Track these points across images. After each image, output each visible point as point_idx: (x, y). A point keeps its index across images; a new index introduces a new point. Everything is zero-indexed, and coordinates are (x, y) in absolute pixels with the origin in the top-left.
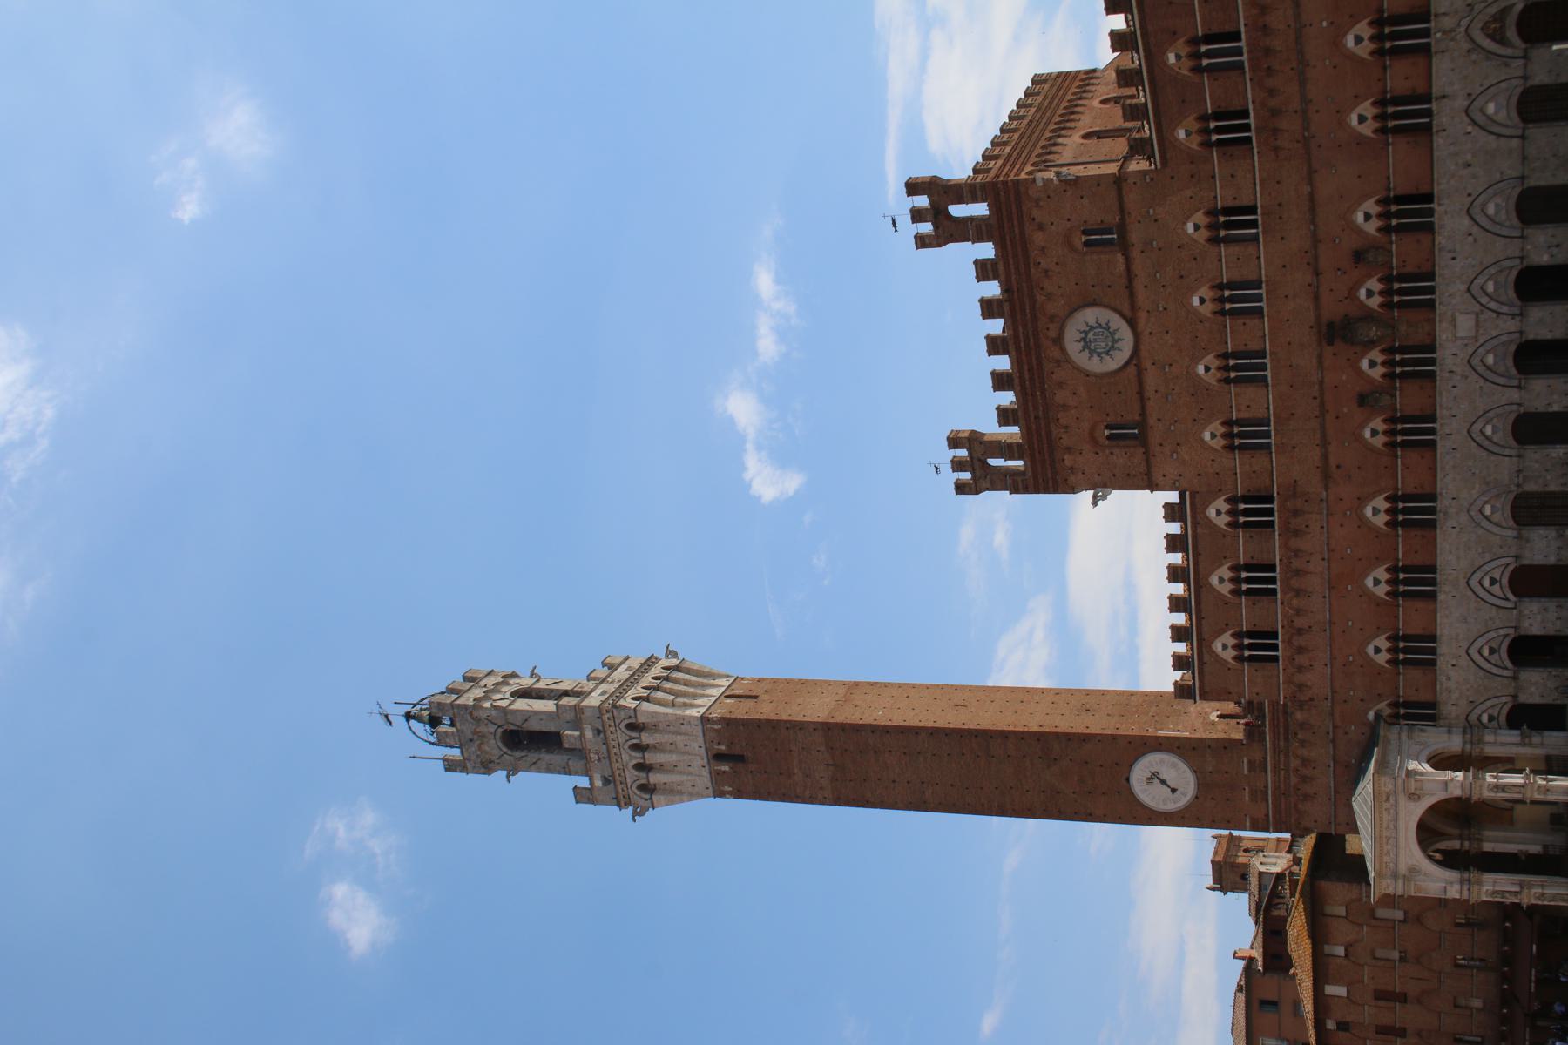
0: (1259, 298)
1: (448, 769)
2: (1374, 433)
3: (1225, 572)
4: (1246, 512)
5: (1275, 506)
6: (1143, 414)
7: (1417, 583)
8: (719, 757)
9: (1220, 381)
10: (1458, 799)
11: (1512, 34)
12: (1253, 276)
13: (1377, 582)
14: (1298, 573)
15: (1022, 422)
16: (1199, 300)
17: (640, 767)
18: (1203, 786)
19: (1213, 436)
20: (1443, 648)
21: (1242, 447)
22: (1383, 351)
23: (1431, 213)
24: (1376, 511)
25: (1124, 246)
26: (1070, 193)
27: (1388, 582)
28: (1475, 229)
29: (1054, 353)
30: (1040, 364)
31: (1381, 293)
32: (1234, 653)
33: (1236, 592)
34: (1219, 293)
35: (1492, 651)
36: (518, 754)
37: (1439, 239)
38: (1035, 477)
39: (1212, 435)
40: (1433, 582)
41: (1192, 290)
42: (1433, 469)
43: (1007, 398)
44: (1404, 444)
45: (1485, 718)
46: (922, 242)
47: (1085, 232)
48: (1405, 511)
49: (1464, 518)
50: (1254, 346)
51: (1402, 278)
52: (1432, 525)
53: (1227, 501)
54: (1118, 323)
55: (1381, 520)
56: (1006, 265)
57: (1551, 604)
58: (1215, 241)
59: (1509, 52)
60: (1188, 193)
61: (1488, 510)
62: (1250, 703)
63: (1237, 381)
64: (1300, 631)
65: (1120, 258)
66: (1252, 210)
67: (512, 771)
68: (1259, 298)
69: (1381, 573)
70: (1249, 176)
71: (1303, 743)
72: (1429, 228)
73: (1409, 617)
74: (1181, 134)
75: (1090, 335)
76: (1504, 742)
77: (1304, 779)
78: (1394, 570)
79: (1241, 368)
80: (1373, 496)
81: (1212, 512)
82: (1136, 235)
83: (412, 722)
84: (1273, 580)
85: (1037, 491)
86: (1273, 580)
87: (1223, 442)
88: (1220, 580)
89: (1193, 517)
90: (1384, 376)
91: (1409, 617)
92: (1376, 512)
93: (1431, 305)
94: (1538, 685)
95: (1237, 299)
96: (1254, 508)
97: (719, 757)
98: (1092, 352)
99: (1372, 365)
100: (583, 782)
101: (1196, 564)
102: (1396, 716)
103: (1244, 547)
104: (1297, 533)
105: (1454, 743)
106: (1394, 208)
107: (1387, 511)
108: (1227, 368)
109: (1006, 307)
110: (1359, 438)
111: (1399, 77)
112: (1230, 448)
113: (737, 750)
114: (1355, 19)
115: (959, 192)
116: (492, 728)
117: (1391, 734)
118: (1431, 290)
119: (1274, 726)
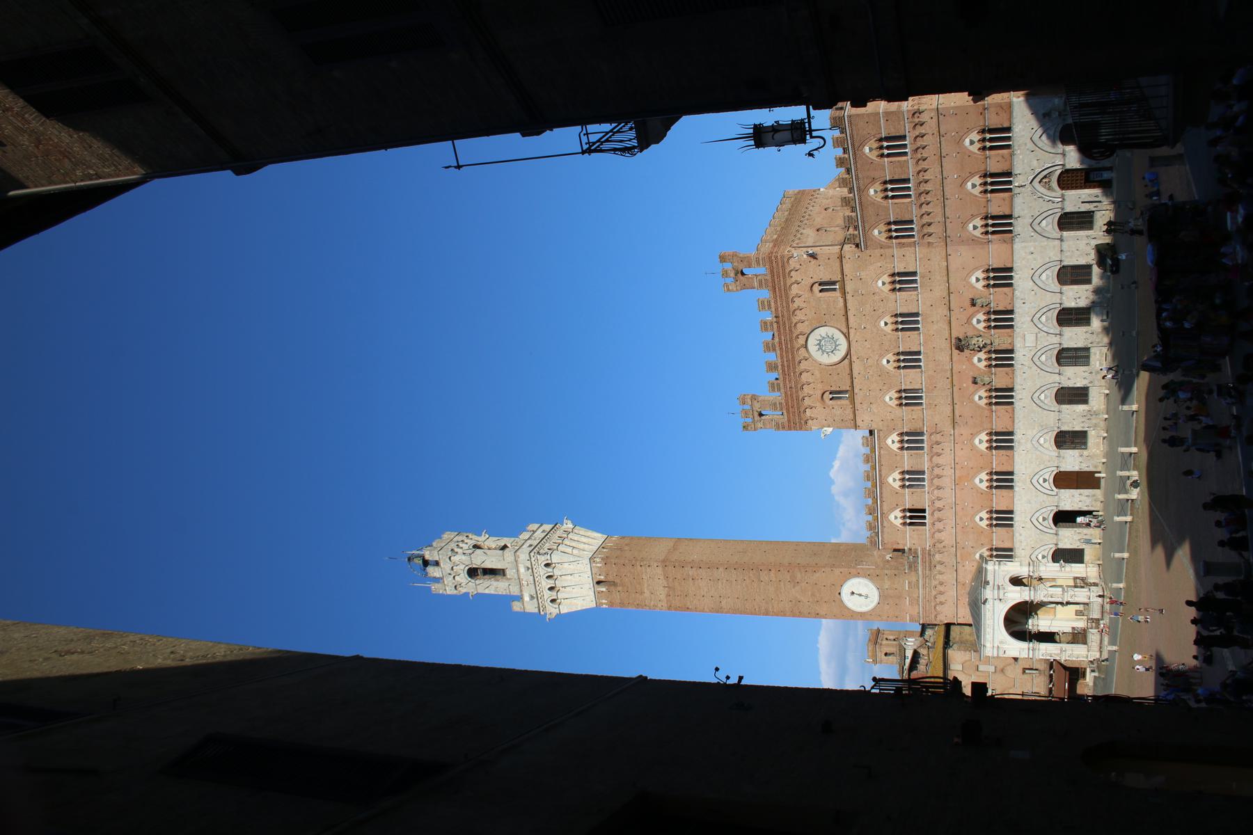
0: (917, 322)
2: (980, 398)
3: (897, 475)
5: (924, 438)
7: (1003, 480)
8: (599, 583)
10: (1026, 602)
11: (1055, 184)
12: (915, 311)
13: (981, 481)
14: (939, 477)
16: (885, 324)
17: (551, 589)
18: (883, 597)
20: (1016, 516)
23: (1011, 278)
24: (981, 442)
25: (844, 293)
28: (1036, 288)
29: (803, 350)
34: (894, 319)
35: (1044, 519)
37: (1016, 292)
38: (789, 421)
39: (890, 398)
40: (1012, 480)
41: (880, 318)
42: (1012, 418)
44: (996, 404)
45: (1040, 557)
49: (1029, 445)
51: (995, 313)
52: (1011, 448)
56: (776, 302)
57: (1076, 492)
58: (894, 290)
59: (1053, 194)
61: (1042, 441)
64: (940, 510)
65: (841, 300)
66: (914, 274)
68: (917, 322)
69: (984, 476)
71: (941, 573)
72: (1010, 285)
73: (1000, 500)
74: (876, 232)
76: (1050, 569)
77: (941, 593)
79: (909, 359)
80: (979, 432)
82: (848, 289)
84: (923, 480)
85: (790, 429)
86: (923, 480)
88: (893, 480)
91: (1000, 500)
93: (1011, 327)
94: (1069, 538)
95: (907, 322)
97: (599, 583)
99: (979, 361)
102: (991, 556)
103: (908, 460)
104: (939, 455)
105: (1022, 571)
106: (992, 275)
108: (899, 361)
109: (775, 325)
110: (973, 401)
111: (997, 205)
112: (901, 405)
113: (610, 578)
114: (972, 175)
115: (747, 261)
116: (462, 567)
117: (990, 567)
118: (1012, 319)
119: (924, 562)
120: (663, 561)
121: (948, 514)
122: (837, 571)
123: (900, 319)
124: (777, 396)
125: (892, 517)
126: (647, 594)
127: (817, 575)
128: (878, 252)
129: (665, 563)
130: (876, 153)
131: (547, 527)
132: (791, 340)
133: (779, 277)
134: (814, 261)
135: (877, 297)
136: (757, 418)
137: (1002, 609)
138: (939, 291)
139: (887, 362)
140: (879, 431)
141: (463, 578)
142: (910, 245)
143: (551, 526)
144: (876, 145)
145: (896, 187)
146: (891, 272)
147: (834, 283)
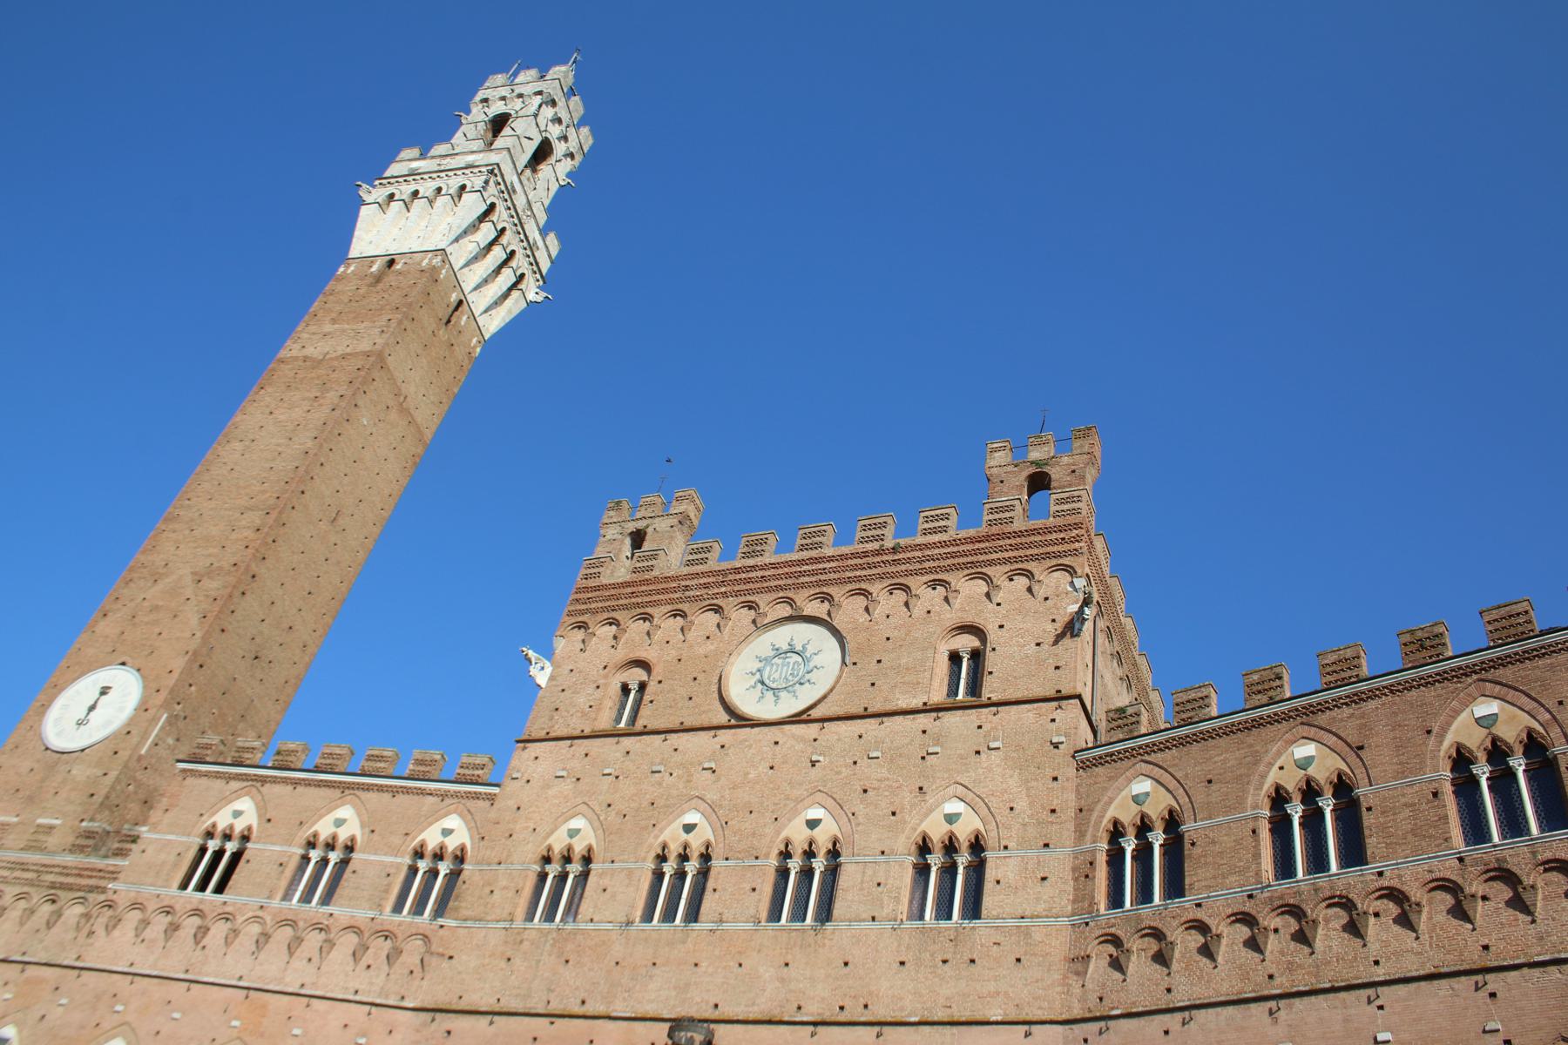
6: (645, 732)
8: (391, 263)
9: (664, 848)
12: (839, 909)
15: (686, 570)
16: (812, 821)
26: (1050, 627)
30: (769, 590)
34: (823, 846)
39: (580, 831)
47: (977, 656)
50: (709, 904)
58: (924, 848)
60: (1021, 804)
65: (916, 703)
70: (1040, 908)
74: (1143, 786)
81: (453, 822)
82: (951, 719)
88: (342, 820)
89: (456, 795)
97: (391, 263)
98: (766, 660)
101: (381, 788)
120: (380, 357)
121: (177, 957)
122: (178, 664)
123: (819, 865)
126: (328, 328)
127: (194, 620)
128: (1067, 799)
129: (379, 359)
130: (1475, 740)
131: (545, 265)
132: (819, 583)
133: (1016, 547)
134: (1051, 630)
135: (907, 797)
136: (631, 527)
138: (896, 994)
139: (687, 828)
140: (491, 798)
141: (497, 108)
142: (1083, 899)
143: (544, 271)
144: (1511, 732)
145: (1331, 821)
146: (990, 840)
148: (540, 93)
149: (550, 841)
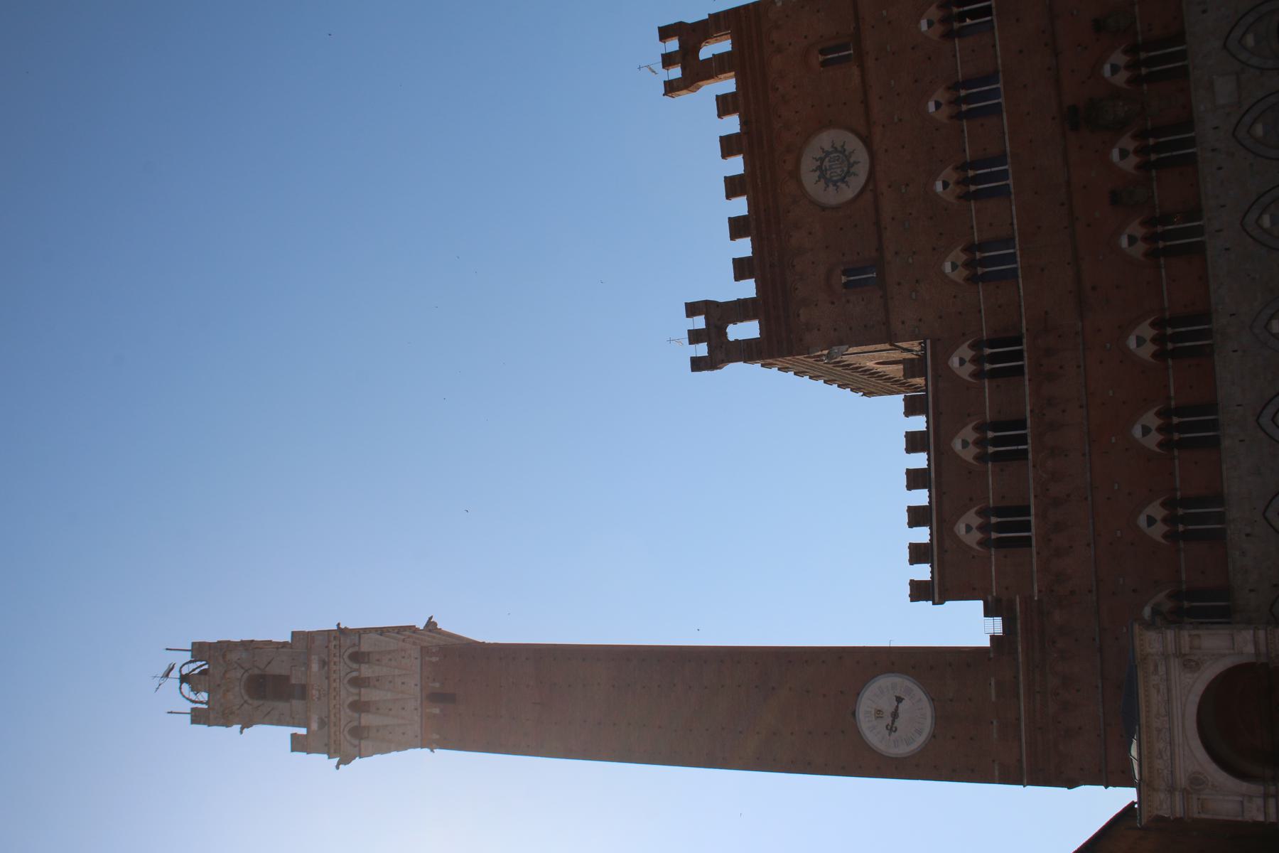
0: (994, 94)
1: (193, 722)
2: (1132, 240)
3: (969, 433)
4: (994, 358)
5: (1025, 347)
9: (959, 197)
13: (1146, 430)
18: (942, 718)
19: (954, 267)
21: (985, 278)
22: (1134, 137)
24: (1140, 341)
27: (1159, 429)
31: (1127, 67)
32: (978, 535)
33: (981, 458)
36: (256, 703)
40: (1214, 425)
43: (744, 247)
46: (671, 88)
48: (1173, 338)
53: (972, 347)
54: (853, 144)
55: (1147, 352)
58: (949, 35)
62: (998, 601)
63: (976, 195)
65: (855, 71)
67: (246, 724)
68: (994, 94)
69: (1151, 419)
75: (826, 163)
78: (1164, 413)
83: (186, 687)
84: (1022, 439)
87: (965, 273)
88: (963, 445)
89: (934, 369)
90: (1138, 167)
92: (1140, 342)
96: (1002, 354)
98: (827, 182)
99: (1122, 156)
100: (303, 731)
107: (1154, 340)
124: (747, 289)
125: (961, 528)
137: (1188, 690)
147: (845, 47)
148: (224, 656)
149: (961, 281)
